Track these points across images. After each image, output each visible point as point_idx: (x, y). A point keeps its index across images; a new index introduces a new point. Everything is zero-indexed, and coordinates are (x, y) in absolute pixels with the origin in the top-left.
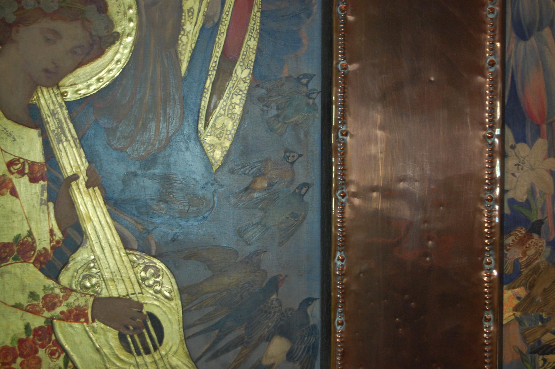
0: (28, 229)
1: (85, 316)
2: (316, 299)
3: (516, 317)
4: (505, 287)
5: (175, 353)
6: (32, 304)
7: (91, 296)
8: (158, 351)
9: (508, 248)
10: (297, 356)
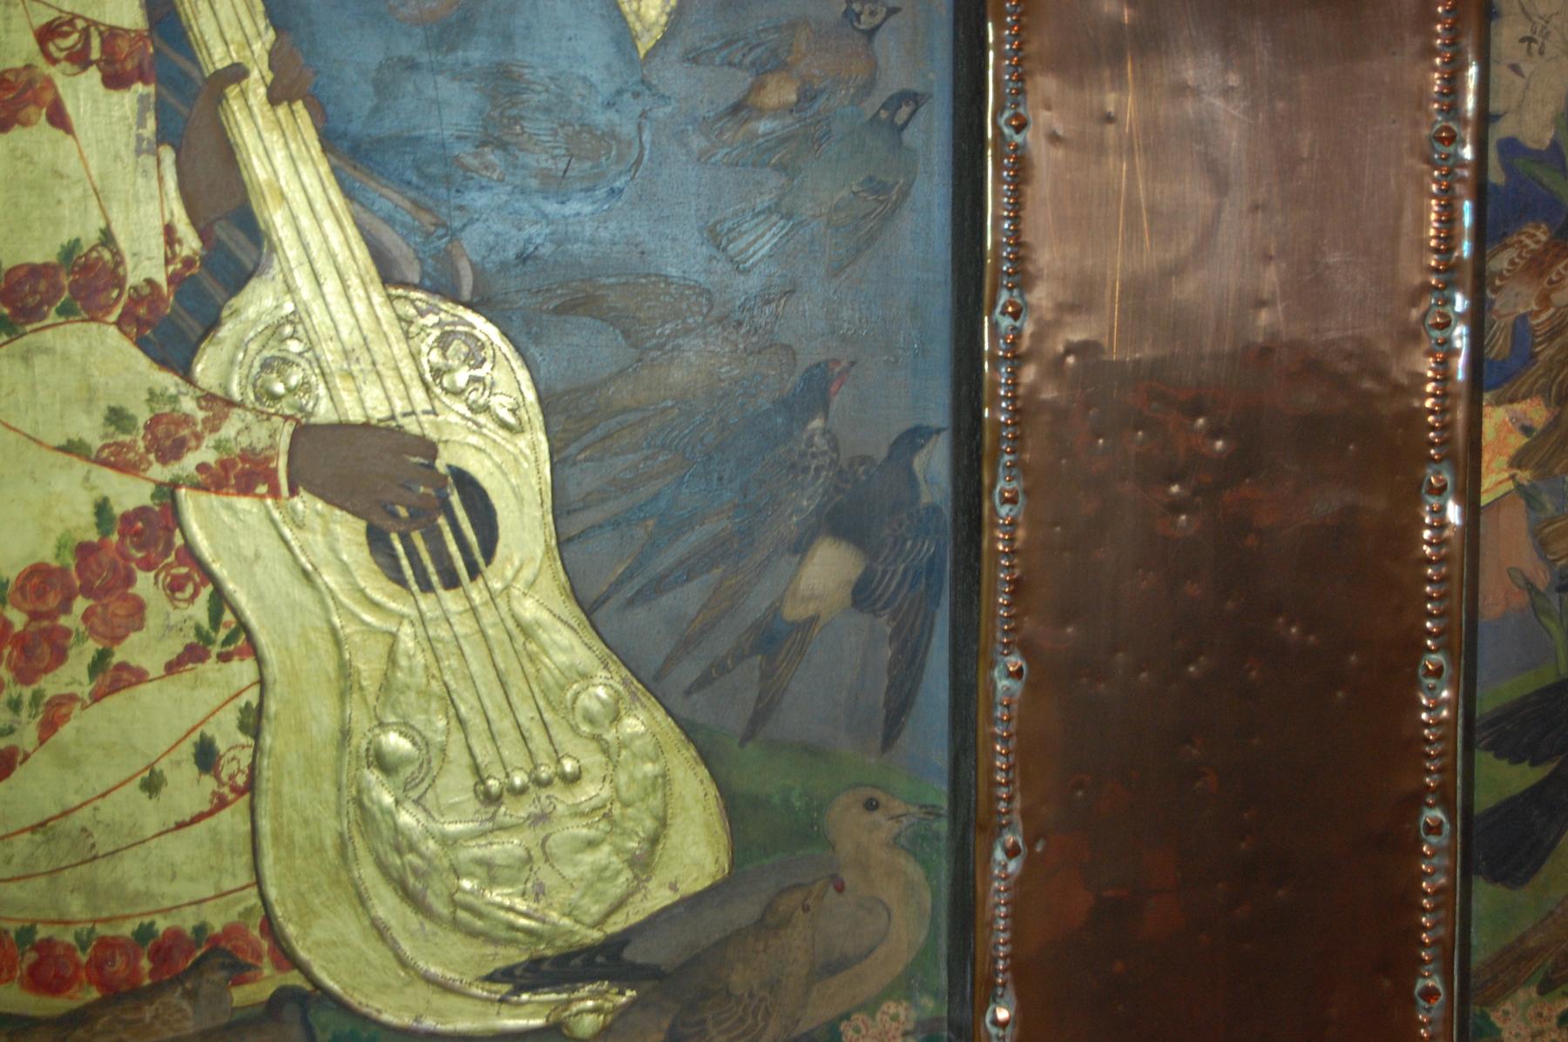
0: (102, 224)
1: (270, 477)
2: (938, 431)
3: (1519, 486)
4: (1487, 396)
5: (531, 584)
6: (116, 444)
7: (286, 418)
8: (480, 581)
9: (1498, 283)
10: (881, 595)
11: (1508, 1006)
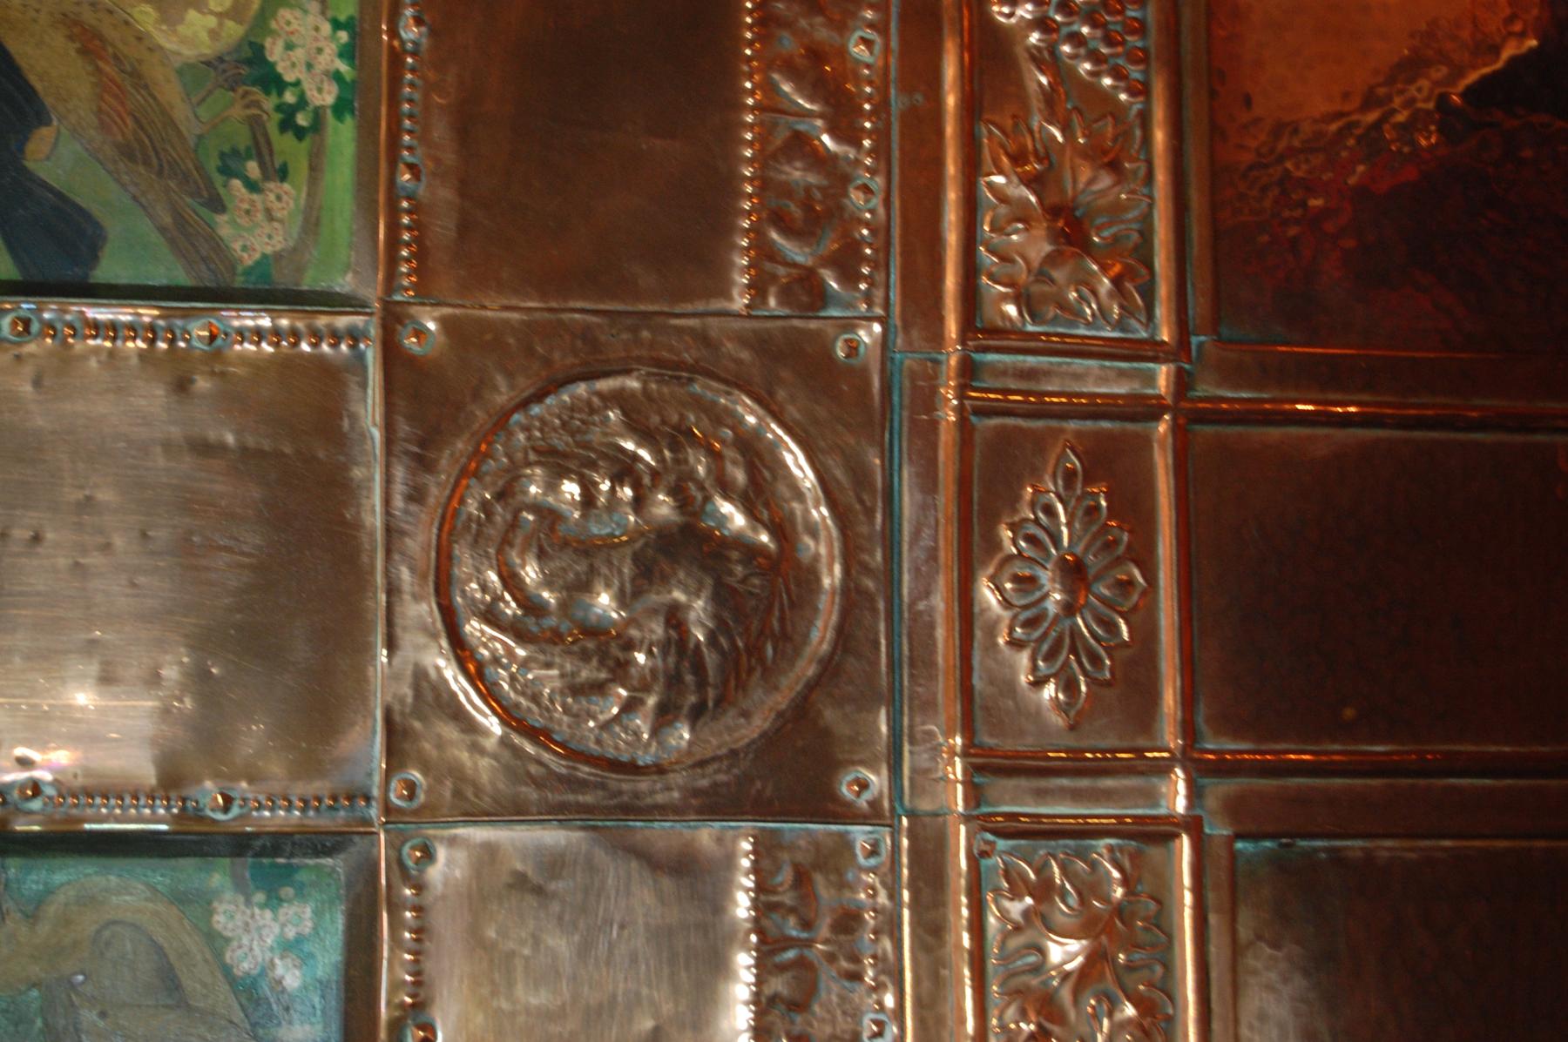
11: (237, 246)
